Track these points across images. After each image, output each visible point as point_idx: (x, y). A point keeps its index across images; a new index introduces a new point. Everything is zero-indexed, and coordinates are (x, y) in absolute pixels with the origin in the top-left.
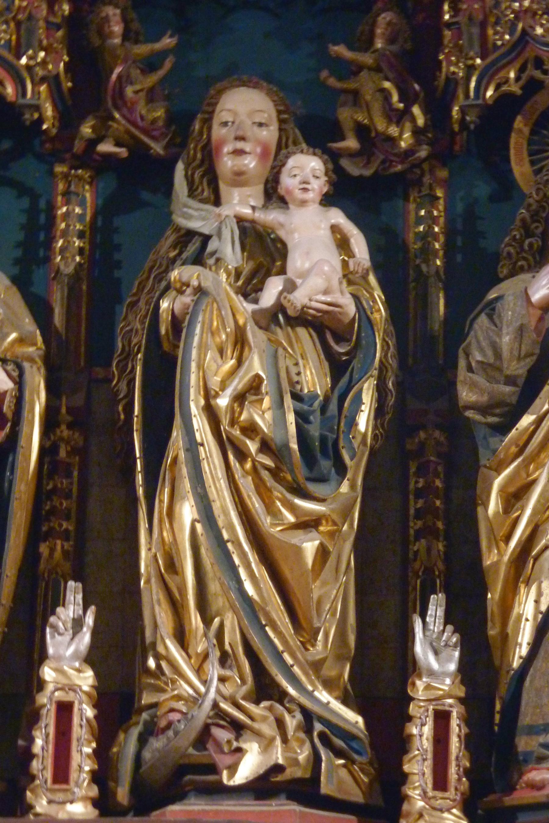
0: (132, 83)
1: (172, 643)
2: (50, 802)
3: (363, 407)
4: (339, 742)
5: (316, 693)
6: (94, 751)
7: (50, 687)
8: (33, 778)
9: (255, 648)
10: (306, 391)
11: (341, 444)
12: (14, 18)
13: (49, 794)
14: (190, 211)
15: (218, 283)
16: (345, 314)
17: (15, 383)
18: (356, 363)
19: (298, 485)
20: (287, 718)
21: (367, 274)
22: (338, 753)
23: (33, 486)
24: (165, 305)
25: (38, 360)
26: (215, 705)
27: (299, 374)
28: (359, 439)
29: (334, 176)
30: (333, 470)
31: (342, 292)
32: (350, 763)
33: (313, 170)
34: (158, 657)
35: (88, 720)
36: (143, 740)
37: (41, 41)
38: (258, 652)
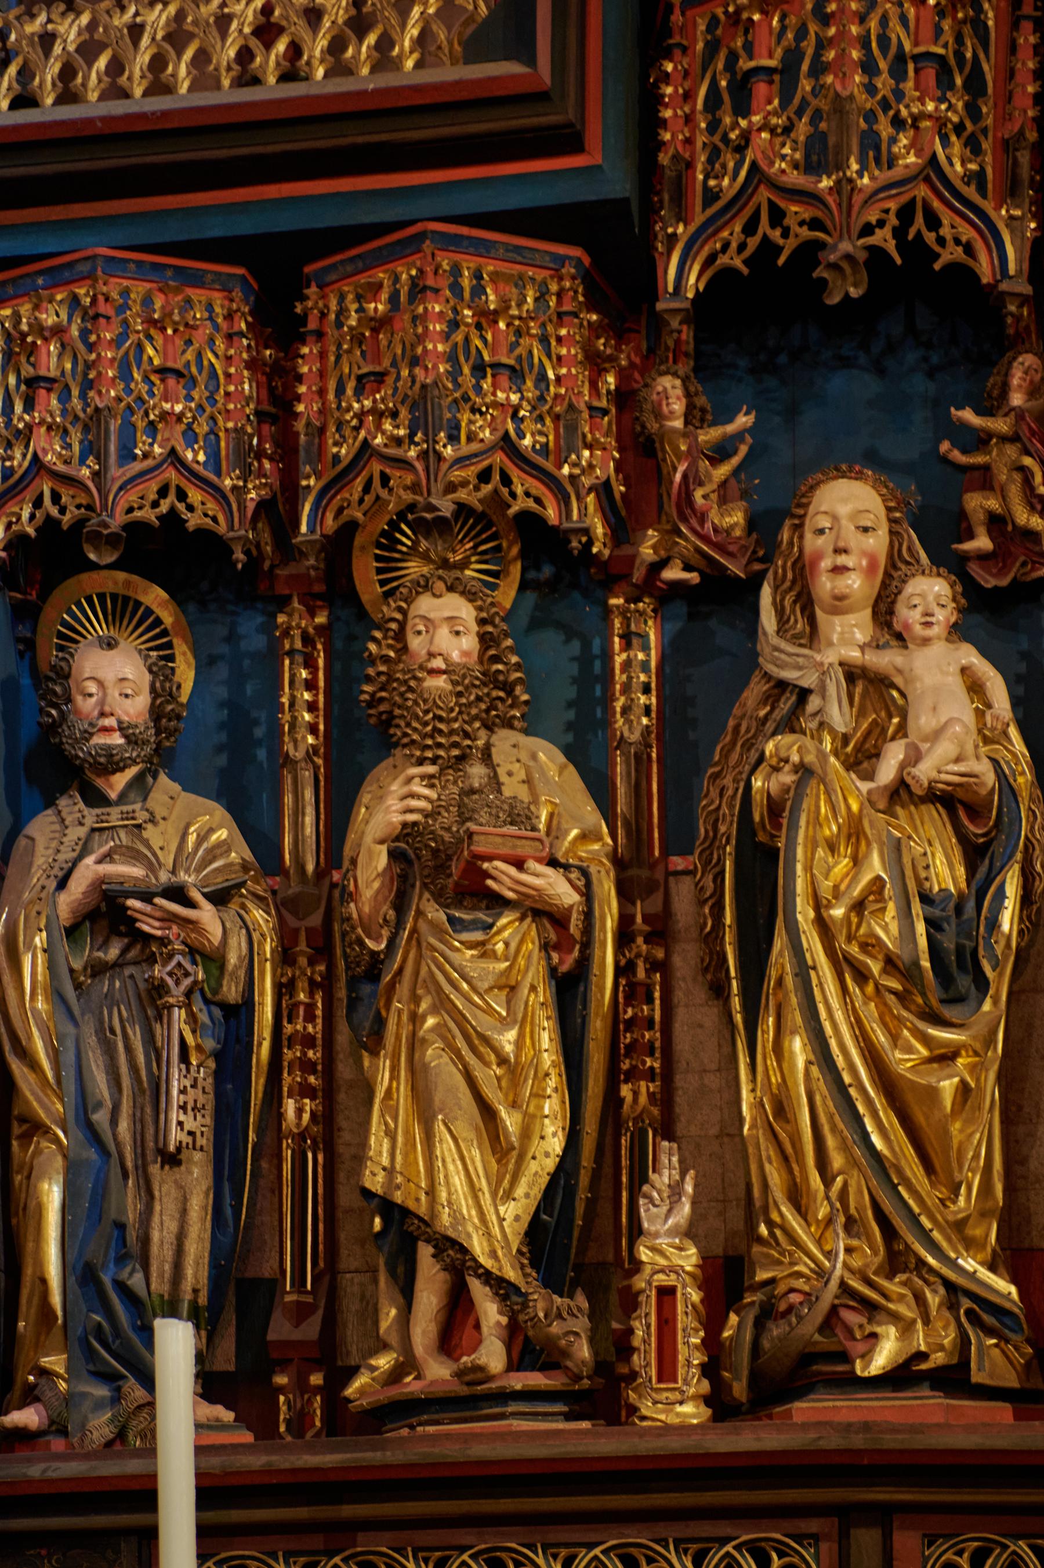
0: (701, 484)
1: (789, 1210)
2: (655, 1403)
3: (1007, 902)
4: (988, 1319)
5: (960, 1261)
6: (703, 1341)
7: (648, 1270)
8: (634, 1375)
9: (887, 1212)
10: (936, 889)
11: (981, 952)
12: (548, 412)
13: (654, 1395)
14: (783, 656)
15: (822, 755)
16: (983, 784)
17: (581, 894)
18: (998, 848)
19: (931, 1008)
20: (929, 1295)
21: (1008, 725)
22: (990, 1332)
23: (609, 1021)
24: (757, 783)
25: (605, 861)
26: (843, 1284)
27: (927, 867)
28: (1003, 942)
29: (963, 601)
30: (973, 987)
31: (978, 758)
32: (1002, 1344)
33: (938, 596)
34: (770, 1224)
35: (693, 1306)
36: (759, 1325)
37: (584, 436)
38: (891, 1217)
